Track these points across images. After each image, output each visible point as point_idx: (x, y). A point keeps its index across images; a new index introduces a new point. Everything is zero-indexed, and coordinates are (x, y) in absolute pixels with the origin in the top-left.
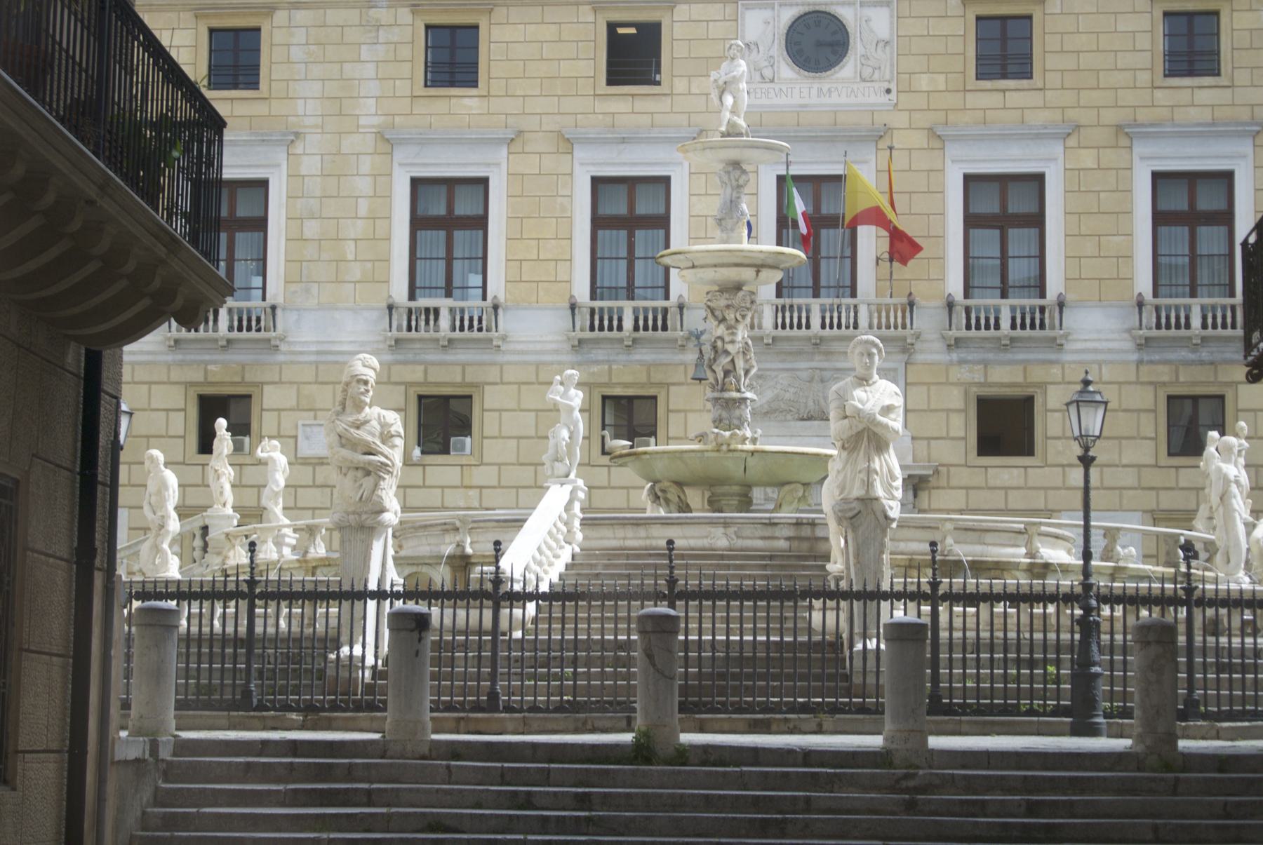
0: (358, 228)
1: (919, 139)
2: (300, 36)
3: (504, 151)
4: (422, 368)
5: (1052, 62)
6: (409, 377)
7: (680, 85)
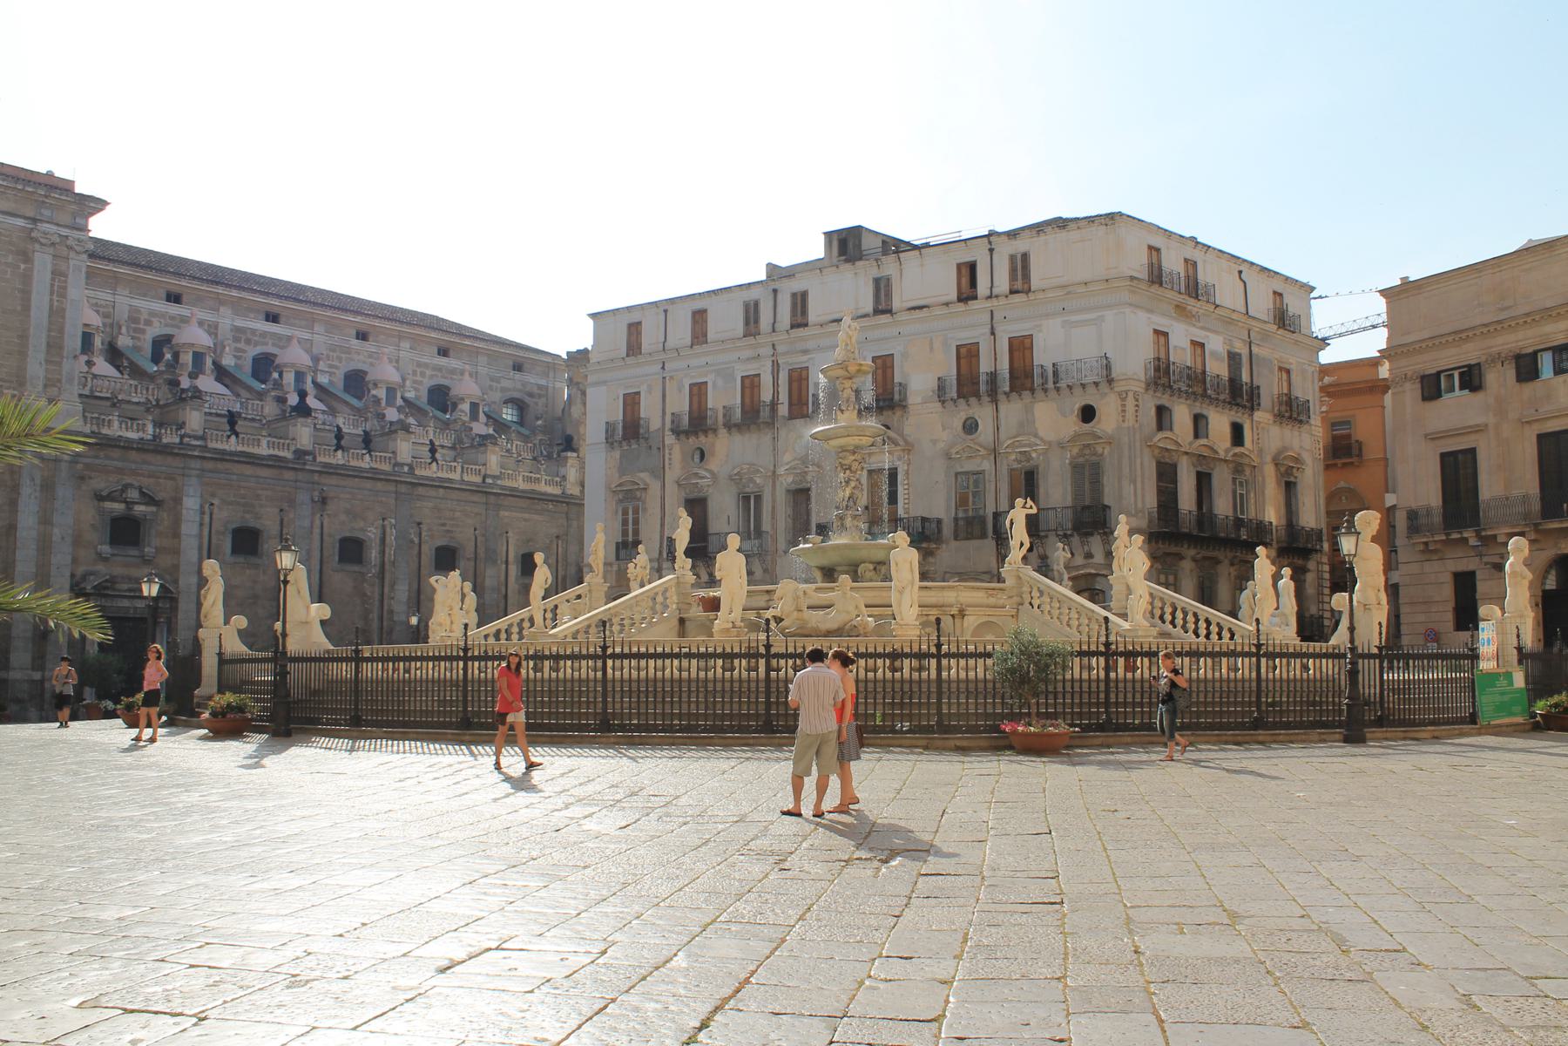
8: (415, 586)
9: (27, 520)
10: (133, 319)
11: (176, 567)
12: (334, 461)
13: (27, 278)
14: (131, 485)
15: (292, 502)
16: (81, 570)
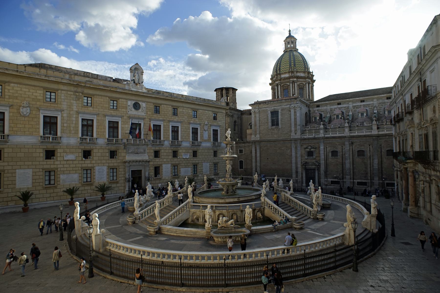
0: (74, 125)
1: (148, 120)
2: (63, 95)
3: (96, 116)
4: (84, 147)
5: (162, 112)
6: (82, 148)
7: (120, 110)
8: (380, 160)
9: (293, 154)
10: (332, 110)
11: (320, 159)
12: (355, 134)
13: (290, 114)
14: (310, 146)
15: (344, 145)
16: (302, 161)
